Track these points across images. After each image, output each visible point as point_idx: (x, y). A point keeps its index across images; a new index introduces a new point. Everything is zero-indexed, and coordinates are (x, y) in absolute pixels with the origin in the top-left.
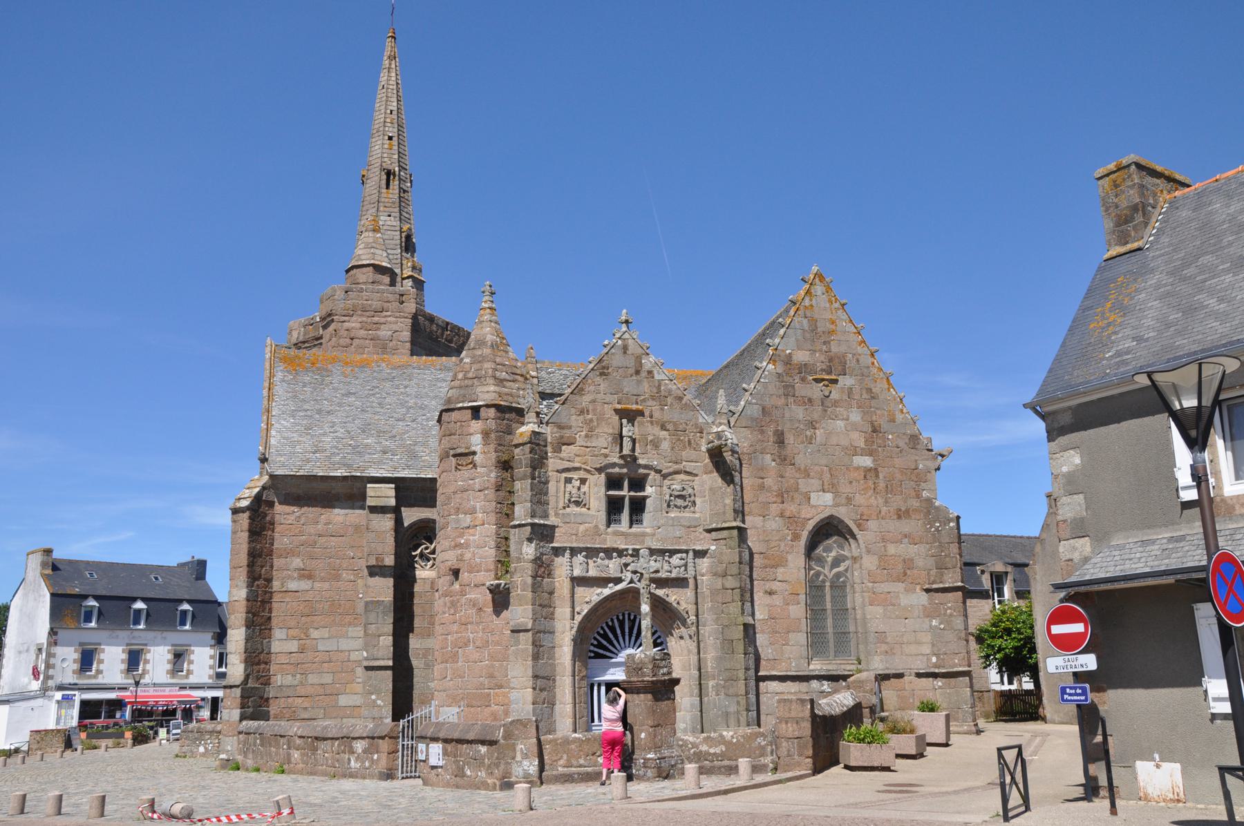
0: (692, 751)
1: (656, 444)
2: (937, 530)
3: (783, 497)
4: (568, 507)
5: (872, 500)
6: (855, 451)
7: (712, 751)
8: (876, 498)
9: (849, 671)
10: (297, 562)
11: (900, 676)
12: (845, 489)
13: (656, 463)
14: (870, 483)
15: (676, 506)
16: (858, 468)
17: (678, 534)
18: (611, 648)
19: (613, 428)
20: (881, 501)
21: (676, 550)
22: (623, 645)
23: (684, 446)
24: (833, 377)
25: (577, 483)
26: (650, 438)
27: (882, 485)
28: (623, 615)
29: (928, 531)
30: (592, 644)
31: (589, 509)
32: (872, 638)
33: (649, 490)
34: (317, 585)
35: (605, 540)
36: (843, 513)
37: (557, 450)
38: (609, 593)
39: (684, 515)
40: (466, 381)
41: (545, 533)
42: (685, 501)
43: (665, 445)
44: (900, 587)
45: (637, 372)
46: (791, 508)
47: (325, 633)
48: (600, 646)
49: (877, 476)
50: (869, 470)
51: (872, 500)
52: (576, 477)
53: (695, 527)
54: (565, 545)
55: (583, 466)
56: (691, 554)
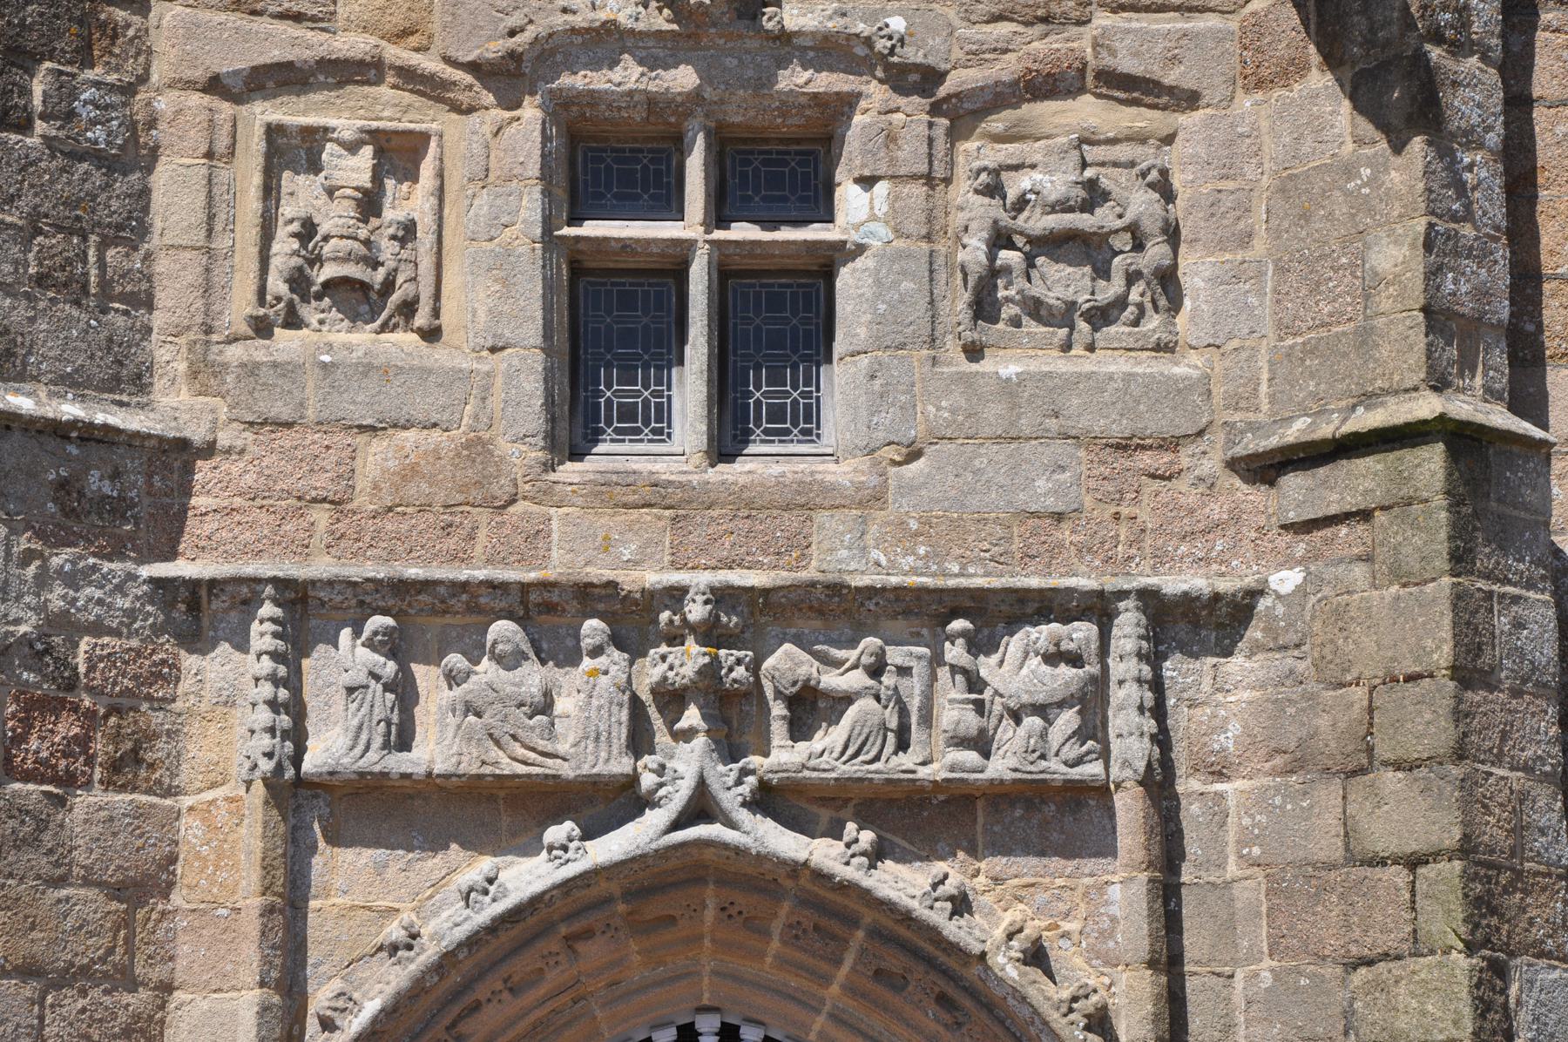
4: (293, 321)
13: (897, 24)
15: (1036, 309)
17: (1043, 491)
21: (1021, 596)
25: (357, 169)
31: (431, 335)
33: (851, 201)
35: (539, 534)
38: (538, 887)
39: (1080, 363)
41: (96, 482)
42: (1102, 272)
52: (345, 125)
53: (1171, 444)
54: (250, 569)
55: (395, 53)
56: (1128, 625)
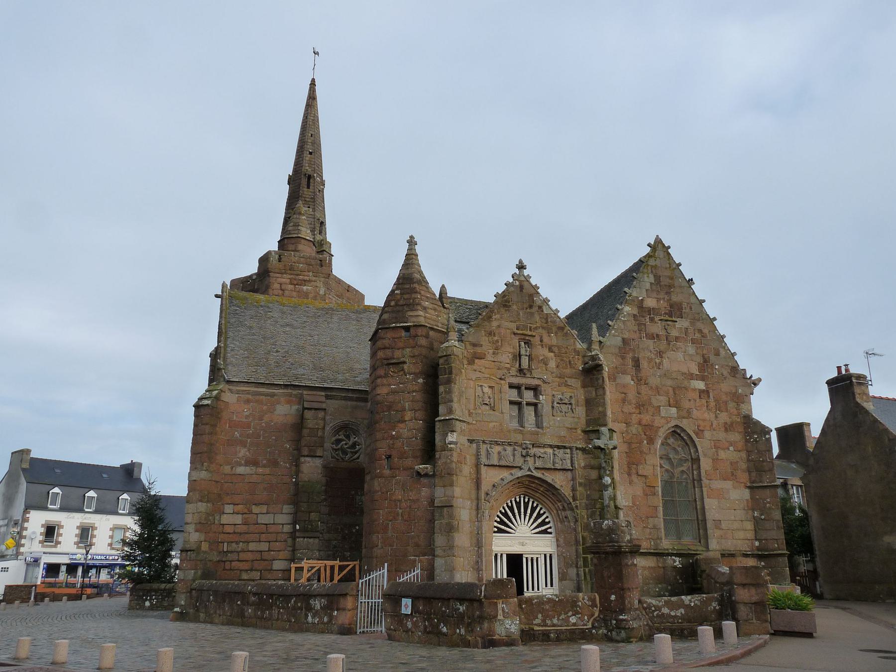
0: (655, 614)
1: (545, 362)
2: (755, 440)
3: (640, 409)
5: (706, 416)
6: (691, 377)
7: (673, 614)
8: (709, 413)
9: (694, 550)
10: (243, 452)
11: (733, 555)
12: (686, 404)
14: (704, 401)
16: (695, 390)
18: (510, 524)
19: (513, 348)
20: (712, 416)
21: (563, 446)
22: (519, 523)
23: (566, 365)
24: (674, 319)
26: (541, 358)
27: (712, 404)
28: (520, 498)
29: (747, 441)
30: (496, 521)
32: (709, 525)
34: (260, 470)
36: (685, 424)
37: (471, 362)
40: (397, 308)
43: (552, 364)
44: (728, 484)
45: (531, 307)
46: (646, 418)
47: (264, 509)
48: (502, 522)
49: (709, 396)
50: (701, 392)
51: (706, 416)
